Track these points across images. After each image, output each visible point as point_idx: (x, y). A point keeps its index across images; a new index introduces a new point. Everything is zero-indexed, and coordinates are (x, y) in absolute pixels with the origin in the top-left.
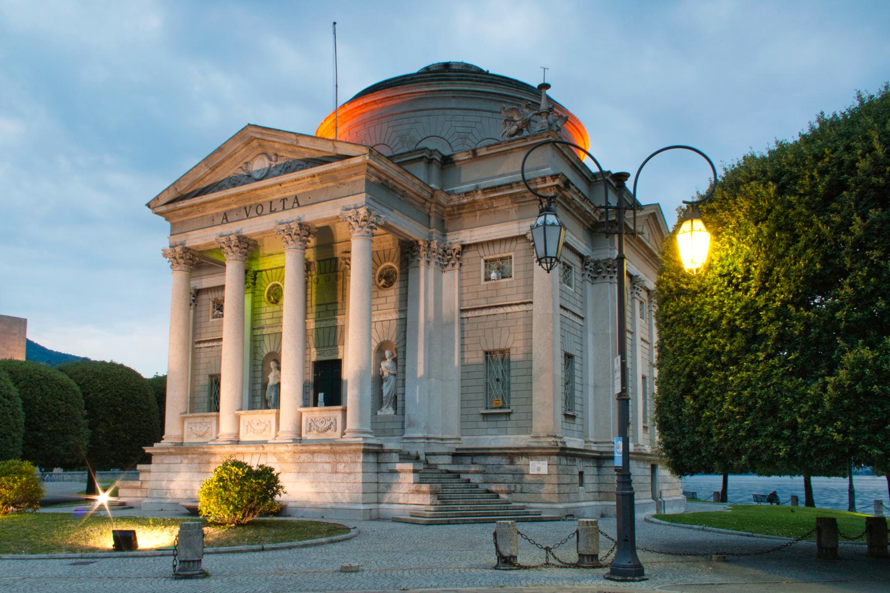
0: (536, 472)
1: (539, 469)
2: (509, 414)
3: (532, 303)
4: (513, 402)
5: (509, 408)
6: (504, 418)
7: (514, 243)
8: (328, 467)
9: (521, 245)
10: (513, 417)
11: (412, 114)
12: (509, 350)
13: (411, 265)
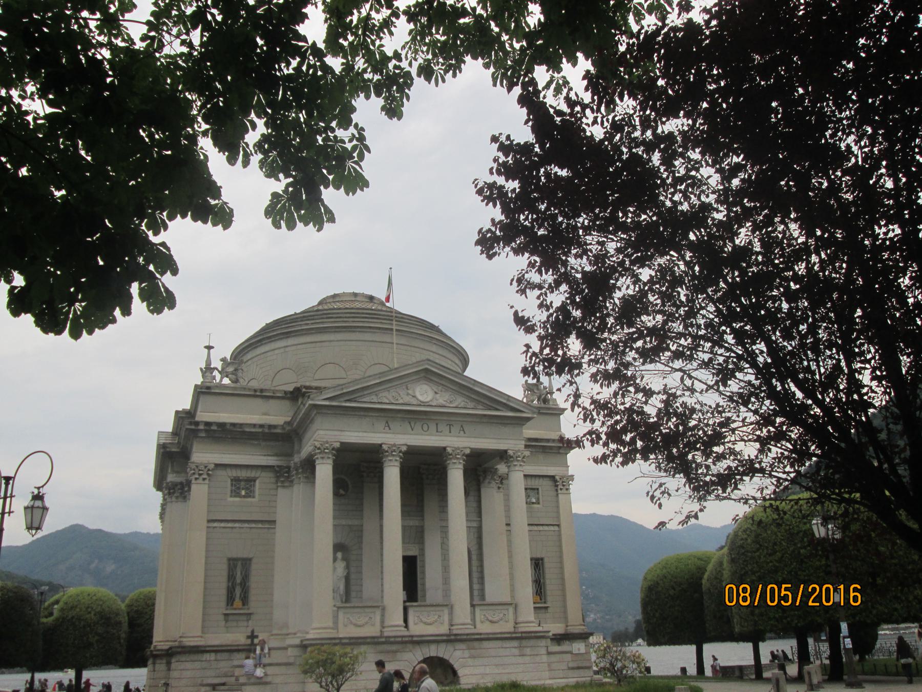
1: (579, 649)
2: (546, 608)
3: (558, 525)
4: (549, 598)
6: (543, 611)
7: (541, 480)
8: (516, 651)
9: (547, 483)
10: (550, 610)
12: (542, 559)
13: (482, 485)
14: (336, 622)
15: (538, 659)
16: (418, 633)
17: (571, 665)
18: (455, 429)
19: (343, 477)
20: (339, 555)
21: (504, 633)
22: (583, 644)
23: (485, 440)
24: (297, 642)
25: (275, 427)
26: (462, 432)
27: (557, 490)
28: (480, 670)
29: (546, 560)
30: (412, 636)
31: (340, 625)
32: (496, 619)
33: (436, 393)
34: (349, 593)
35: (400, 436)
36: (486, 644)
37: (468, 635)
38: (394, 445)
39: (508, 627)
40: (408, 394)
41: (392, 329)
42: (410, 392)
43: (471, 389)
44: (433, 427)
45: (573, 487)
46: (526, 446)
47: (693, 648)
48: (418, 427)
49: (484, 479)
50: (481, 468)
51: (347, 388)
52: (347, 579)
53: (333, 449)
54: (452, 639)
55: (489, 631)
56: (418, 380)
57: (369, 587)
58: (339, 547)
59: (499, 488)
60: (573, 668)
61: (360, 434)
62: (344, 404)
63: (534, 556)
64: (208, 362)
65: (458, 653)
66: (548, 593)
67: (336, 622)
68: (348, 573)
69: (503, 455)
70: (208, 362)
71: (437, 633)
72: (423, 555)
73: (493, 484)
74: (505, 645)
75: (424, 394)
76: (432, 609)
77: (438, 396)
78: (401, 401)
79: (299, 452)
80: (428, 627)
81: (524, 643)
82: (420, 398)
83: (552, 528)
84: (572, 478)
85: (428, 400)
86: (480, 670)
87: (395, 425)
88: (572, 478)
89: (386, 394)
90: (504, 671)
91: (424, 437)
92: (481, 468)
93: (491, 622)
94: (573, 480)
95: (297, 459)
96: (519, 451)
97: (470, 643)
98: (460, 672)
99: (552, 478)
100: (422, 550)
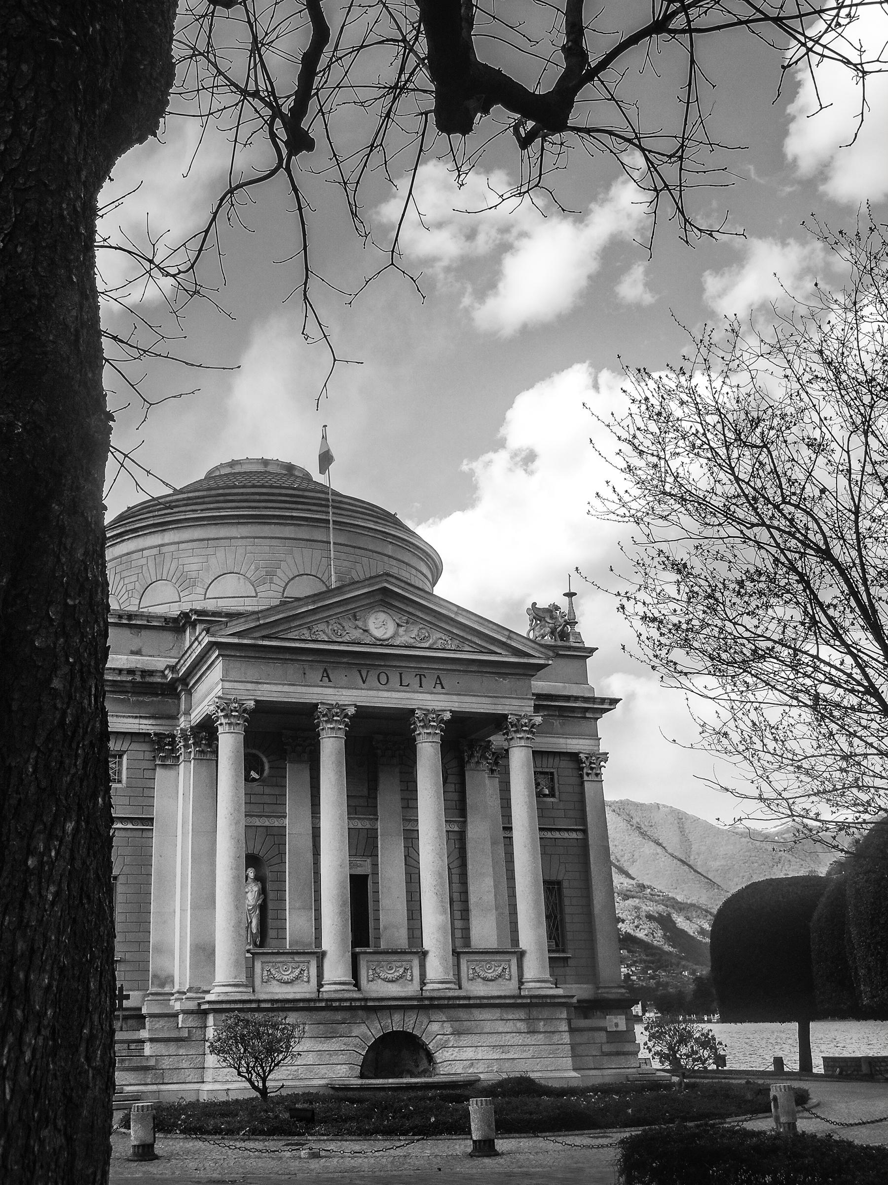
0: (615, 1029)
1: (617, 1025)
5: (564, 951)
7: (557, 759)
8: (521, 1026)
9: (565, 764)
10: (570, 962)
11: (352, 550)
12: (559, 883)
13: (467, 767)
14: (251, 975)
15: (556, 1038)
16: (374, 995)
17: (606, 1048)
18: (428, 682)
19: (254, 751)
20: (251, 873)
21: (505, 997)
22: (624, 1017)
23: (474, 699)
24: (192, 1005)
25: (151, 673)
26: (438, 686)
27: (581, 776)
28: (469, 1053)
29: (565, 884)
30: (366, 1000)
31: (258, 981)
33: (398, 625)
34: (263, 934)
35: (345, 692)
36: (477, 1014)
37: (449, 998)
38: (338, 706)
39: (508, 988)
40: (356, 627)
42: (360, 623)
43: (452, 619)
44: (395, 679)
45: (606, 772)
46: (537, 708)
47: (794, 1027)
48: (372, 679)
49: (471, 756)
51: (265, 617)
52: (263, 908)
53: (245, 711)
54: (427, 1005)
55: (482, 994)
56: (371, 607)
57: (294, 924)
58: (252, 860)
59: (492, 771)
60: (609, 1054)
61: (286, 688)
62: (260, 642)
63: (547, 878)
65: (435, 1027)
66: (569, 936)
67: (251, 975)
68: (265, 901)
69: (498, 722)
71: (403, 995)
72: (375, 873)
74: (505, 1016)
76: (395, 958)
77: (401, 630)
78: (347, 638)
79: (187, 713)
80: (390, 985)
81: (535, 1013)
82: (378, 633)
83: (574, 835)
84: (605, 757)
85: (385, 637)
86: (469, 1053)
87: (338, 675)
88: (605, 757)
89: (322, 626)
90: (504, 1056)
91: (381, 694)
93: (484, 979)
95: (183, 723)
96: (525, 716)
97: (453, 1013)
99: (574, 757)
100: (375, 865)
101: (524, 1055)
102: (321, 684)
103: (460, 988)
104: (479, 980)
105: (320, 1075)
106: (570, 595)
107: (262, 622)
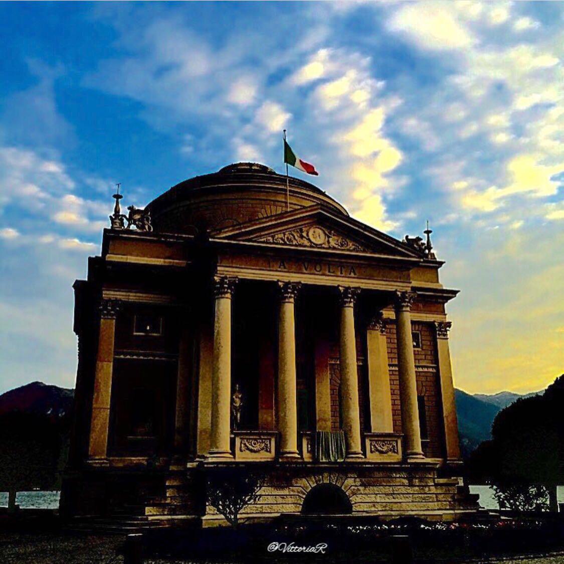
32: (385, 449)
41: (286, 190)
50: (370, 307)
56: (311, 225)
57: (266, 417)
59: (382, 332)
64: (117, 211)
65: (350, 481)
70: (117, 211)
73: (378, 327)
75: (317, 237)
83: (431, 370)
84: (449, 325)
88: (449, 325)
92: (370, 307)
94: (450, 326)
98: (353, 499)
101: (407, 500)
102: (279, 269)
103: (366, 457)
104: (377, 453)
105: (276, 511)
106: (428, 232)
107: (243, 230)
